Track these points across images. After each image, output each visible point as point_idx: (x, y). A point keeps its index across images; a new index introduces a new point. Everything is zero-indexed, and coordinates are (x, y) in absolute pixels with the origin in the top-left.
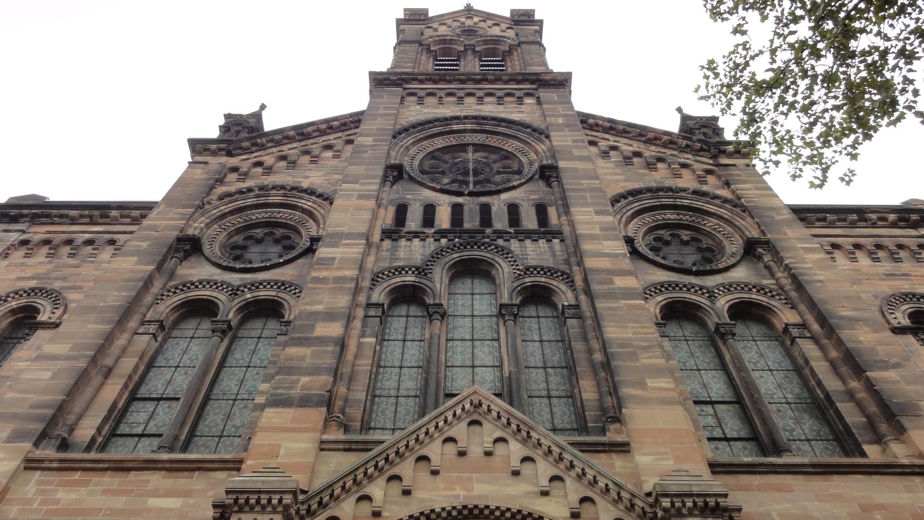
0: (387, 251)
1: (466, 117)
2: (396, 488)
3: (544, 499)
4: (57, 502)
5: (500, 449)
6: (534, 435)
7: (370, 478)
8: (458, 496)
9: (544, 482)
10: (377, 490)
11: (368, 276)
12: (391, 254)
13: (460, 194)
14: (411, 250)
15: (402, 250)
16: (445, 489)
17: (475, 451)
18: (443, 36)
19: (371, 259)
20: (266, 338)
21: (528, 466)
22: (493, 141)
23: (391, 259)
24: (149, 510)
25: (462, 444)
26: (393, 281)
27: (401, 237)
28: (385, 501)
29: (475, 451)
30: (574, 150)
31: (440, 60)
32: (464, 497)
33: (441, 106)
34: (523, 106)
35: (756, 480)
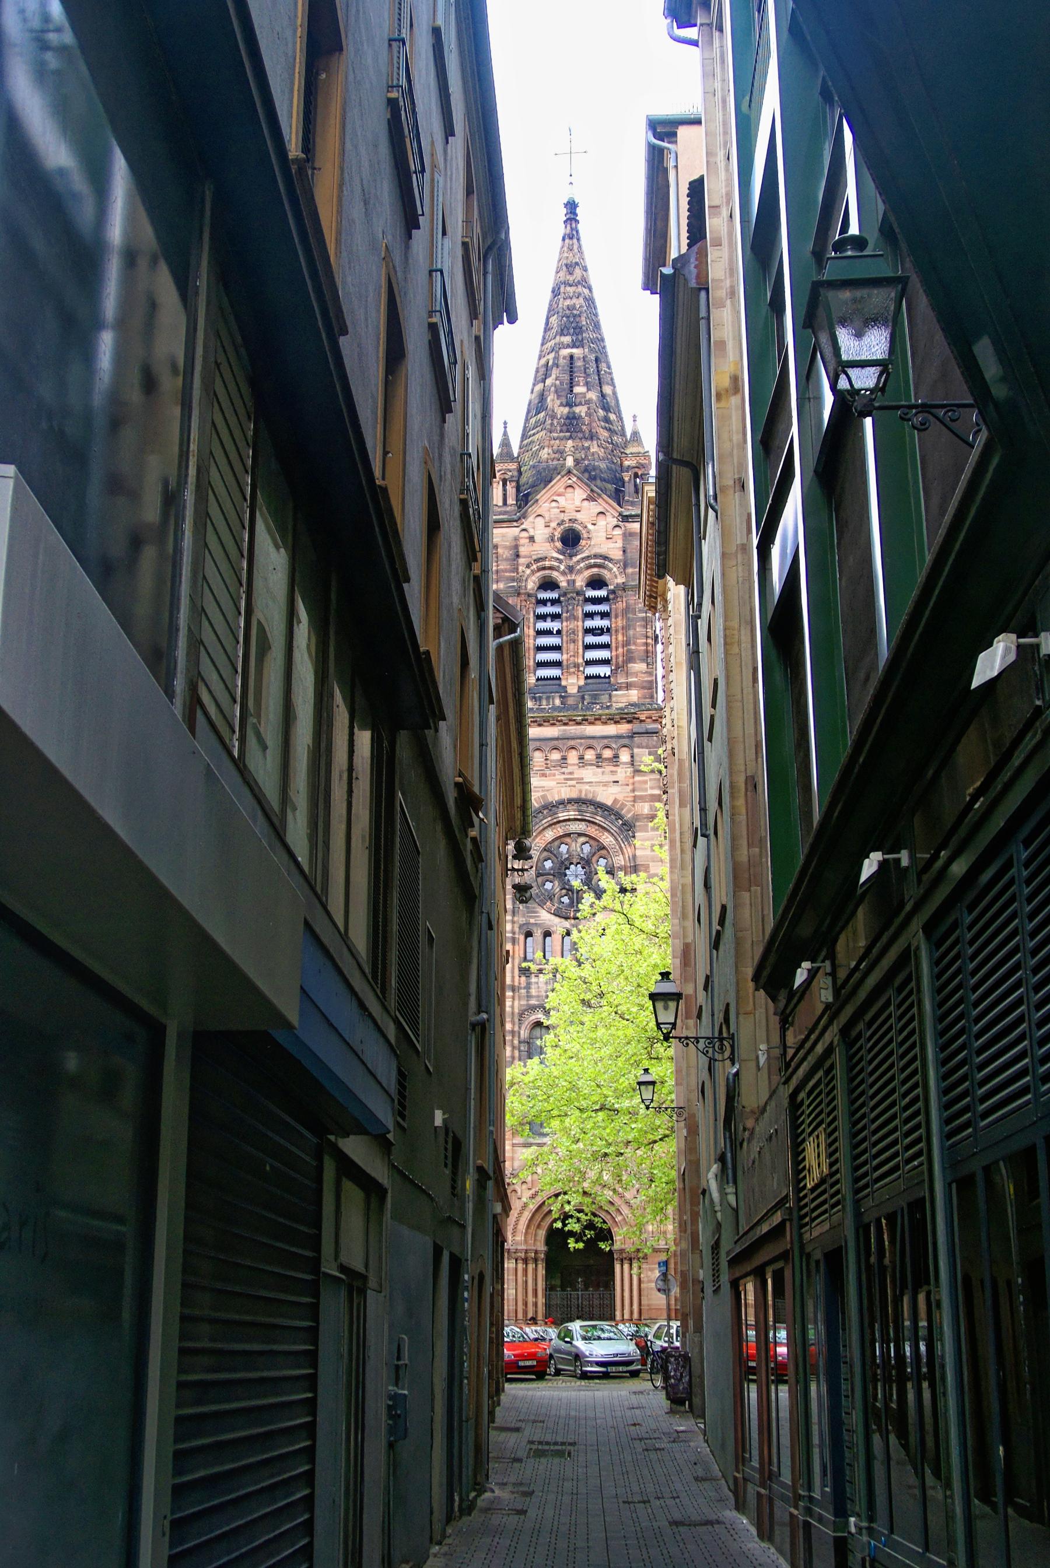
0: (524, 988)
1: (570, 801)
11: (516, 1020)
12: (528, 992)
13: (567, 918)
14: (538, 987)
15: (533, 987)
18: (544, 559)
19: (516, 1003)
22: (592, 831)
23: (528, 996)
26: (531, 1018)
27: (531, 973)
30: (651, 864)
31: (543, 602)
33: (548, 772)
34: (619, 770)
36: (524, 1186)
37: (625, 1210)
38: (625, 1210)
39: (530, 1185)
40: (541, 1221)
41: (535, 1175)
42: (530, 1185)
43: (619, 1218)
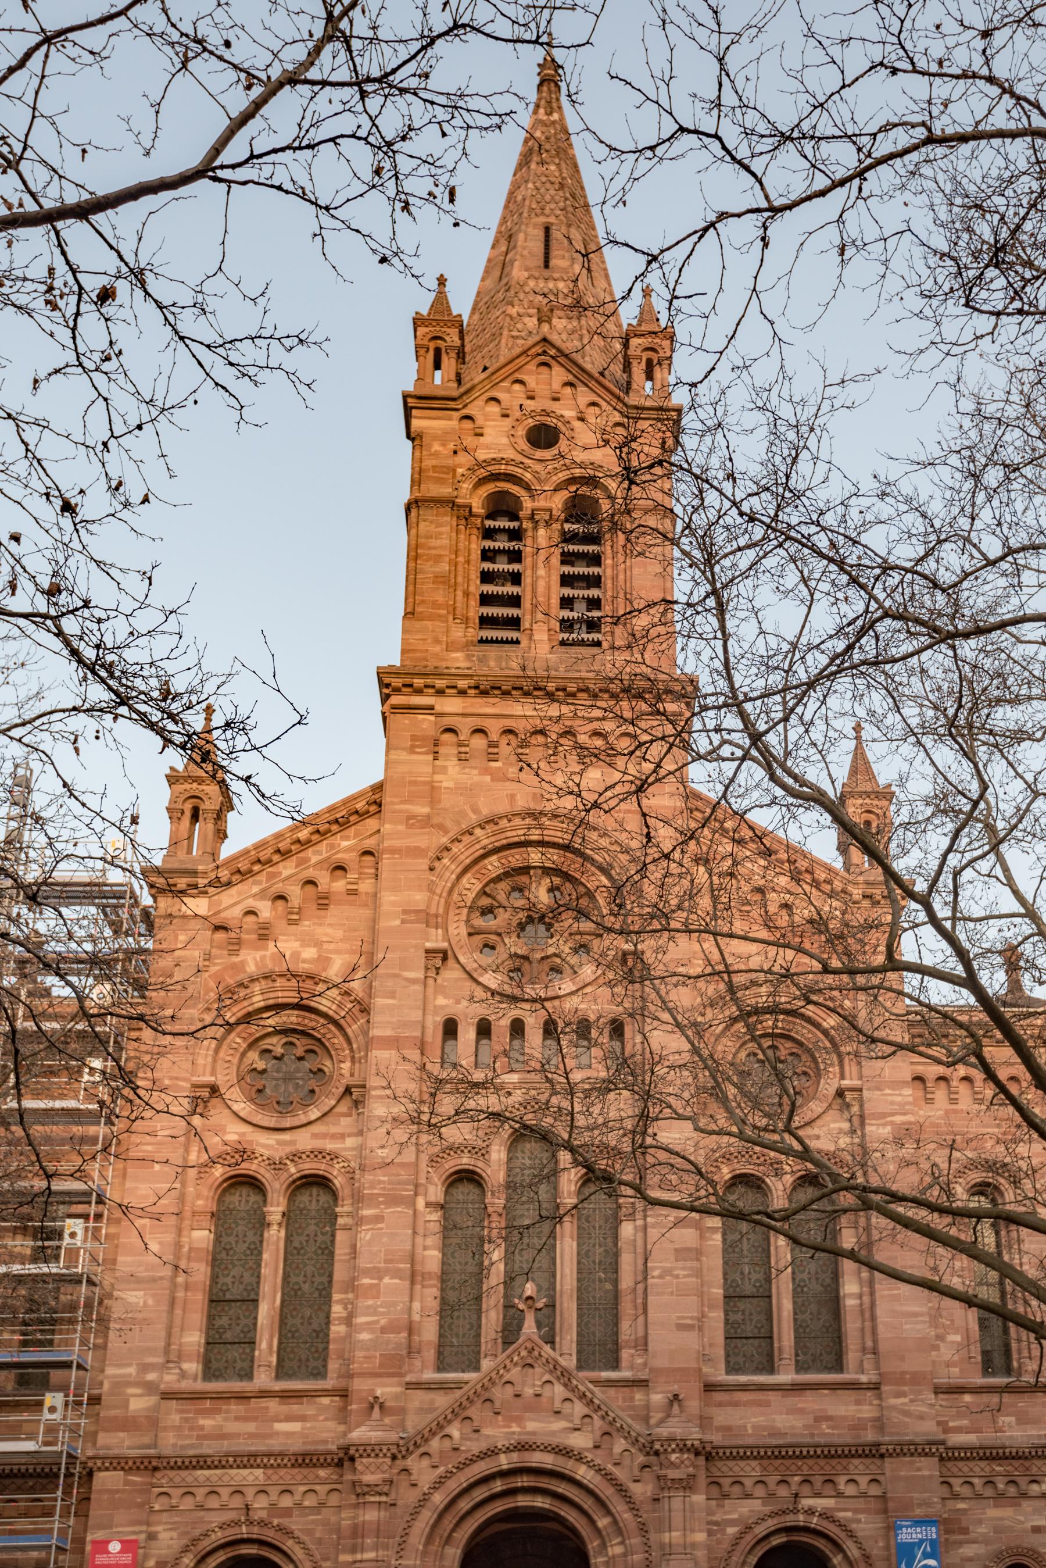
2: (468, 1428)
3: (577, 1433)
4: (202, 1428)
5: (547, 1391)
6: (575, 1382)
7: (450, 1422)
8: (514, 1433)
9: (577, 1421)
10: (454, 1430)
16: (504, 1427)
17: (529, 1391)
20: (28, 746)
21: (568, 1404)
24: (277, 1433)
25: (518, 1388)
28: (462, 1438)
29: (529, 1391)
32: (520, 1434)
35: (745, 1396)
36: (425, 1462)
37: (619, 1507)
38: (619, 1507)
39: (436, 1460)
40: (453, 1530)
41: (447, 1440)
42: (436, 1460)
43: (603, 1522)
